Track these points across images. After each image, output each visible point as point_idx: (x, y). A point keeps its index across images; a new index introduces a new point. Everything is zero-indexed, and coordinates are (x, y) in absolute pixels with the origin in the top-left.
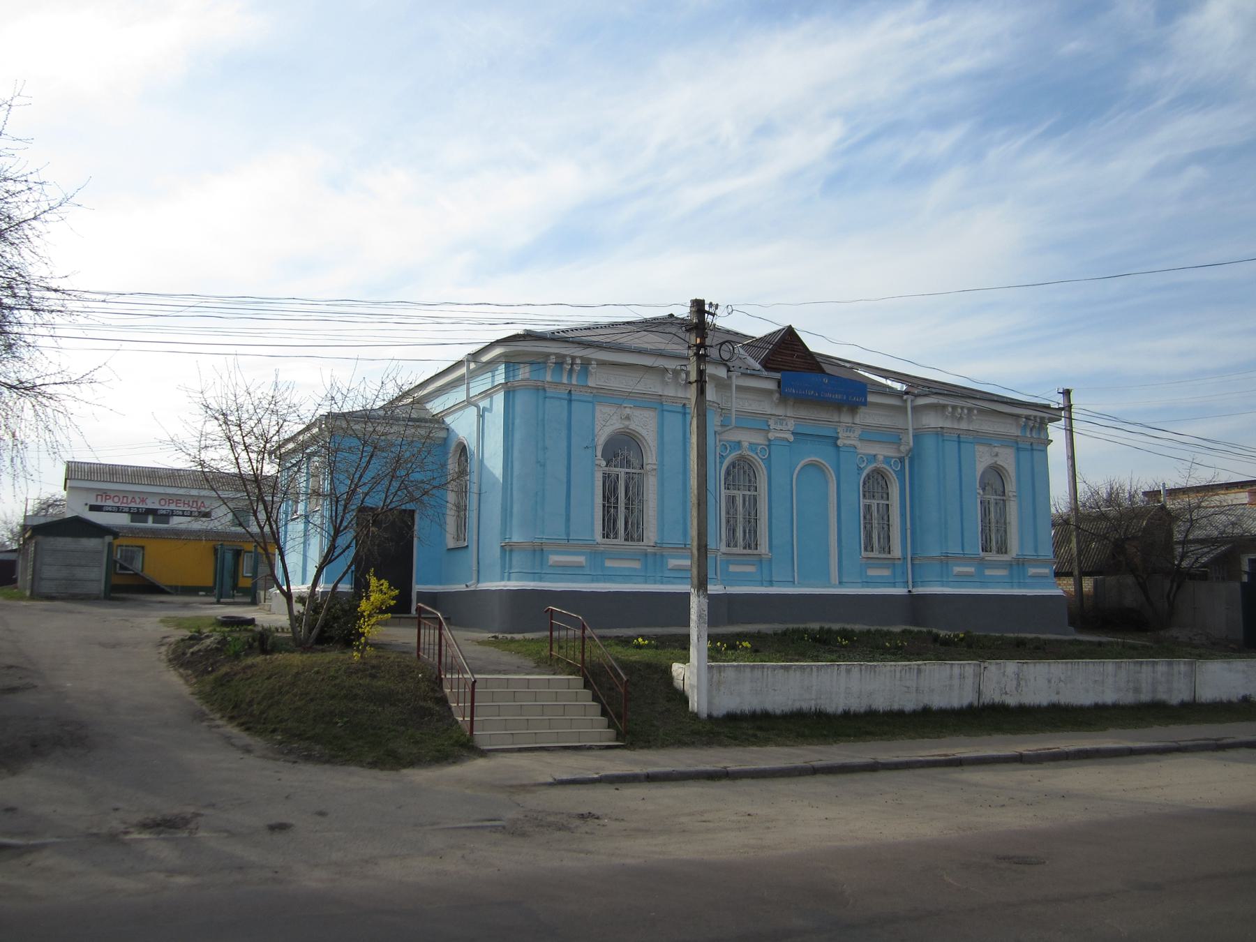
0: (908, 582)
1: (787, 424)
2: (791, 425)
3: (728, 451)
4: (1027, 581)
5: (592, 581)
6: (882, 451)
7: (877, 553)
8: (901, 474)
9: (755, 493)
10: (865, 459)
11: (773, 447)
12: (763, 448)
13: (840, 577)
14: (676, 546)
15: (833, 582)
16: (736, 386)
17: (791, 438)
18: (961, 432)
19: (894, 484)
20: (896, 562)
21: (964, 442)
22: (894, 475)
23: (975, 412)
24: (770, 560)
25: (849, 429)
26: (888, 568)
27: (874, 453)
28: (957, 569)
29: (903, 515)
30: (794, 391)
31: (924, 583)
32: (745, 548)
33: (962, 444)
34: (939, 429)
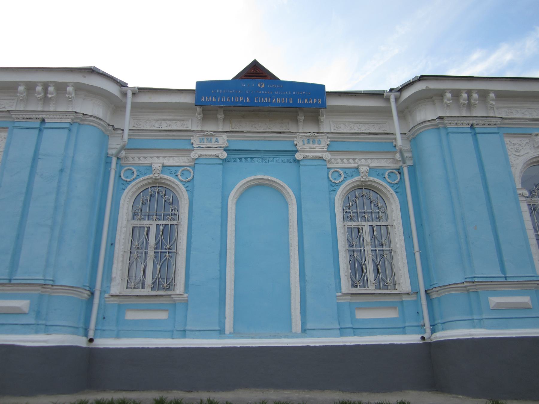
0: (424, 325)
1: (217, 141)
2: (223, 140)
3: (135, 176)
7: (374, 288)
8: (399, 188)
9: (175, 222)
10: (341, 172)
11: (196, 166)
12: (185, 170)
13: (303, 323)
15: (294, 331)
16: (133, 103)
17: (225, 155)
18: (474, 121)
19: (392, 201)
20: (405, 298)
21: (479, 133)
22: (390, 188)
23: (492, 95)
24: (186, 303)
25: (311, 139)
26: (395, 308)
28: (494, 300)
29: (408, 236)
30: (214, 100)
31: (446, 324)
32: (152, 289)
33: (478, 135)
34: (438, 121)
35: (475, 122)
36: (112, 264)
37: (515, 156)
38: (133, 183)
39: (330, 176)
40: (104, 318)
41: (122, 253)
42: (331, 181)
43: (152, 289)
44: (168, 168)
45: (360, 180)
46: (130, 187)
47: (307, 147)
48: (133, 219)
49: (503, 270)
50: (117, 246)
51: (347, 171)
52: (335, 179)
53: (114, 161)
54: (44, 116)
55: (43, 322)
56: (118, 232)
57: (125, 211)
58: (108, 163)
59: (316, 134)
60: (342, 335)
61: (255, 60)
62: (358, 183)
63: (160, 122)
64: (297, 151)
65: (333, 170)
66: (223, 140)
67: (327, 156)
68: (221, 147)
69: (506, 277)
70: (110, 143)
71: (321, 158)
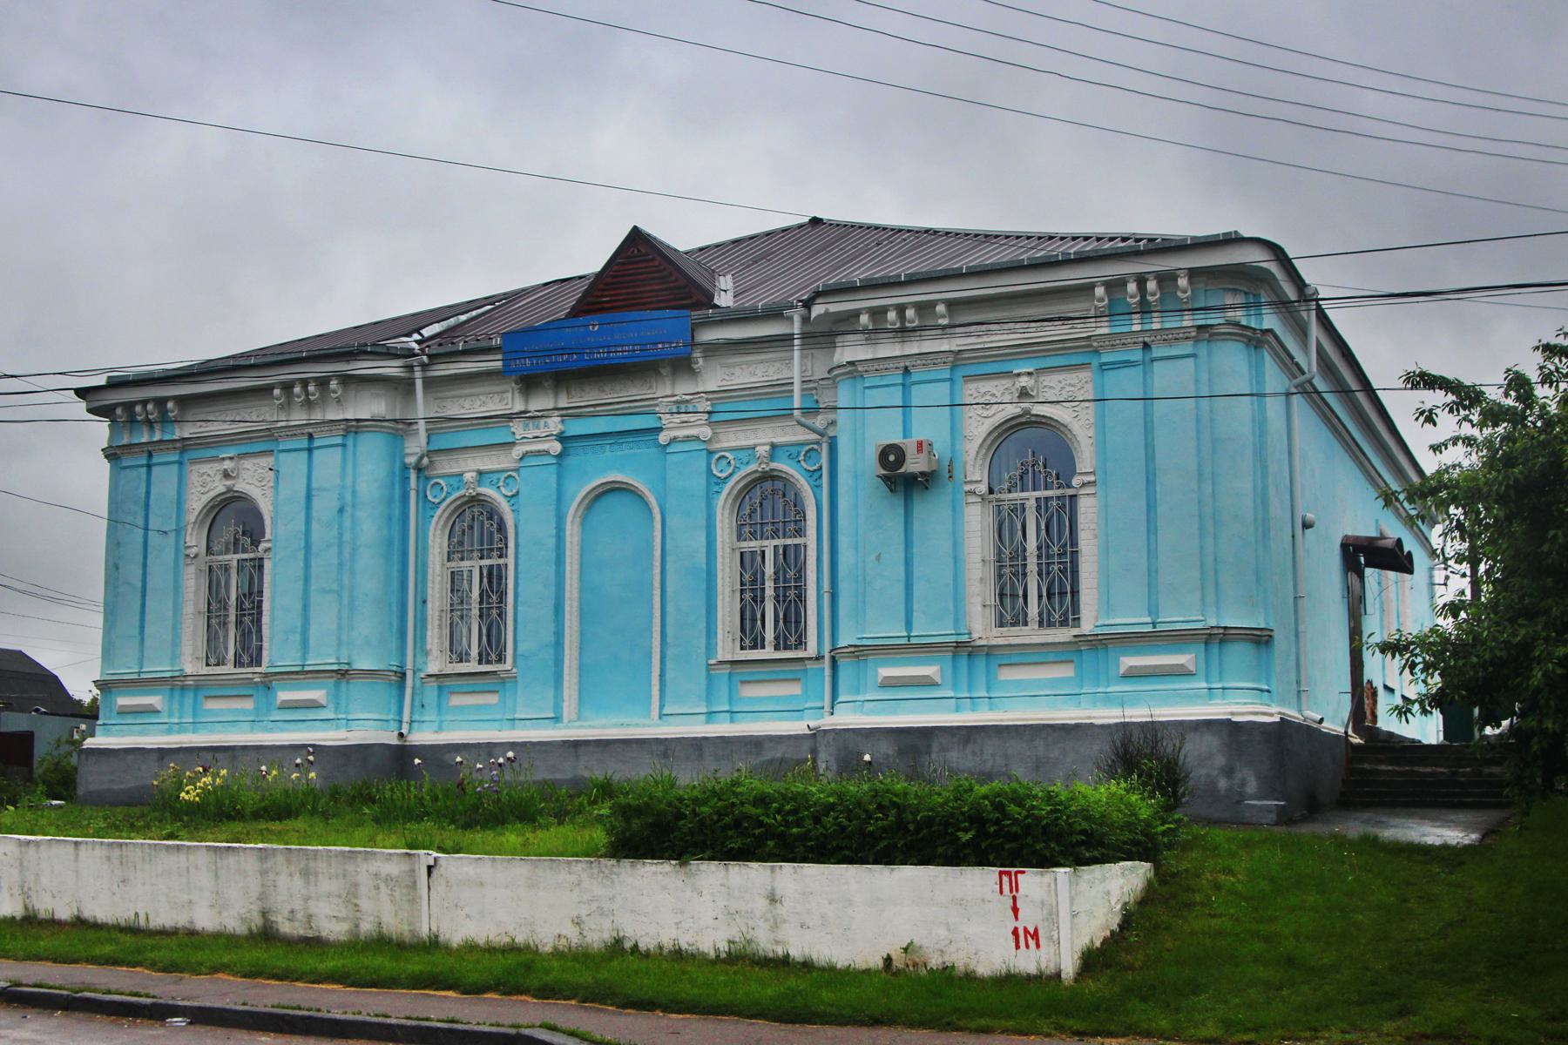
4: (1109, 690)
5: (169, 731)
6: (762, 437)
13: (661, 707)
14: (288, 669)
17: (556, 447)
25: (681, 407)
27: (751, 442)
32: (480, 662)
35: (908, 364)
36: (426, 629)
37: (979, 419)
38: (443, 506)
39: (713, 467)
40: (423, 706)
41: (437, 613)
42: (715, 475)
43: (480, 662)
44: (487, 476)
45: (757, 471)
46: (439, 512)
47: (677, 419)
48: (449, 560)
49: (909, 624)
50: (429, 605)
51: (740, 454)
52: (722, 471)
53: (413, 475)
54: (311, 430)
55: (343, 716)
56: (430, 584)
57: (437, 550)
58: (405, 479)
59: (688, 397)
60: (708, 722)
61: (635, 227)
62: (757, 475)
63: (470, 398)
64: (660, 430)
65: (717, 456)
66: (554, 425)
67: (706, 432)
68: (552, 435)
69: (909, 637)
70: (406, 445)
71: (697, 438)
